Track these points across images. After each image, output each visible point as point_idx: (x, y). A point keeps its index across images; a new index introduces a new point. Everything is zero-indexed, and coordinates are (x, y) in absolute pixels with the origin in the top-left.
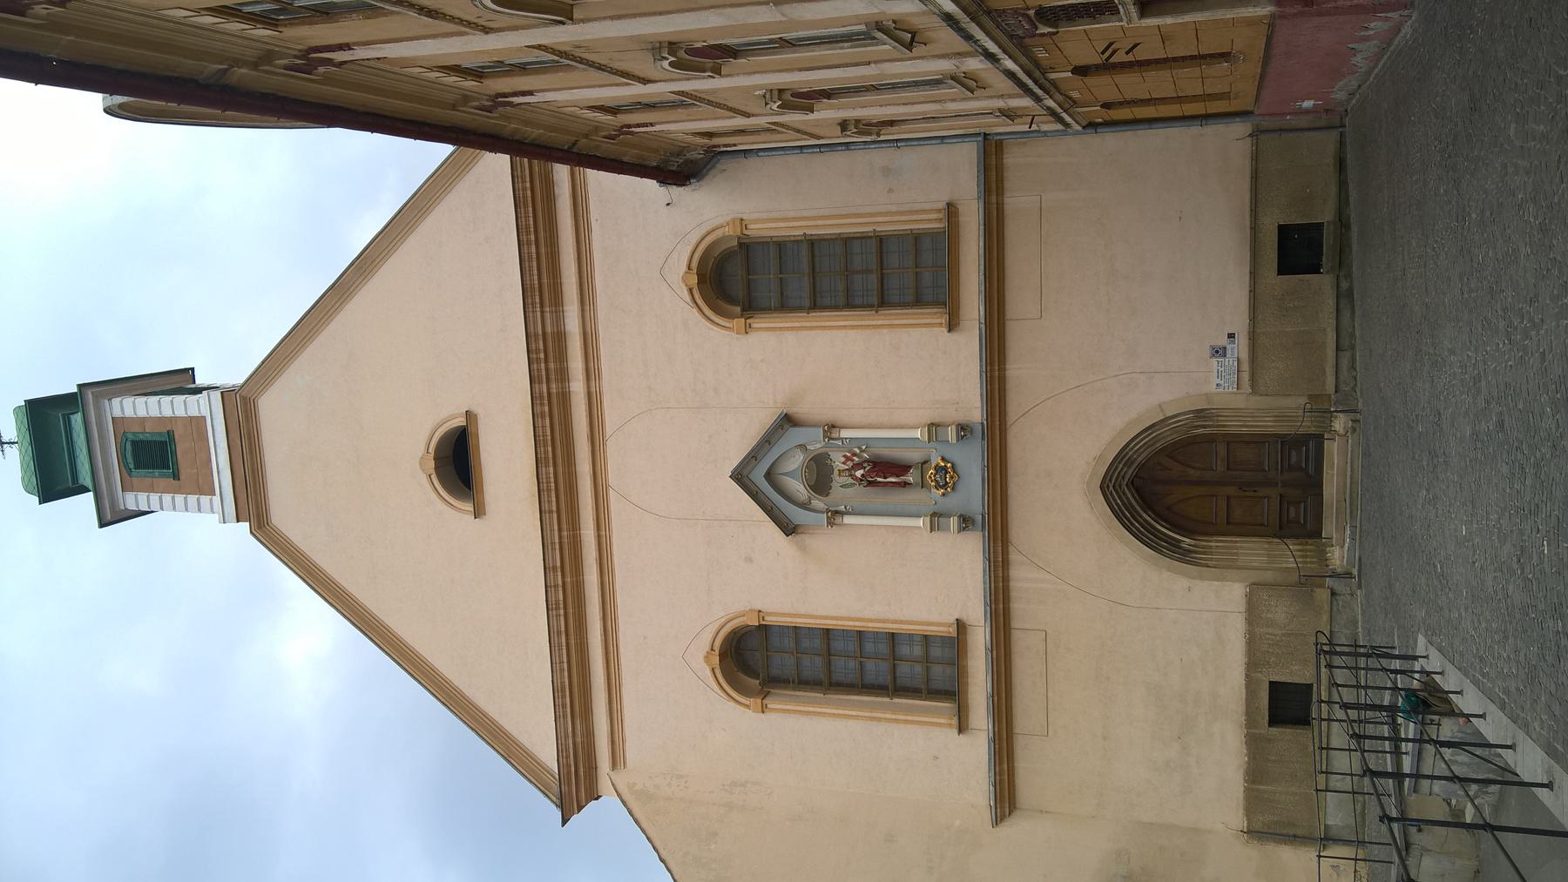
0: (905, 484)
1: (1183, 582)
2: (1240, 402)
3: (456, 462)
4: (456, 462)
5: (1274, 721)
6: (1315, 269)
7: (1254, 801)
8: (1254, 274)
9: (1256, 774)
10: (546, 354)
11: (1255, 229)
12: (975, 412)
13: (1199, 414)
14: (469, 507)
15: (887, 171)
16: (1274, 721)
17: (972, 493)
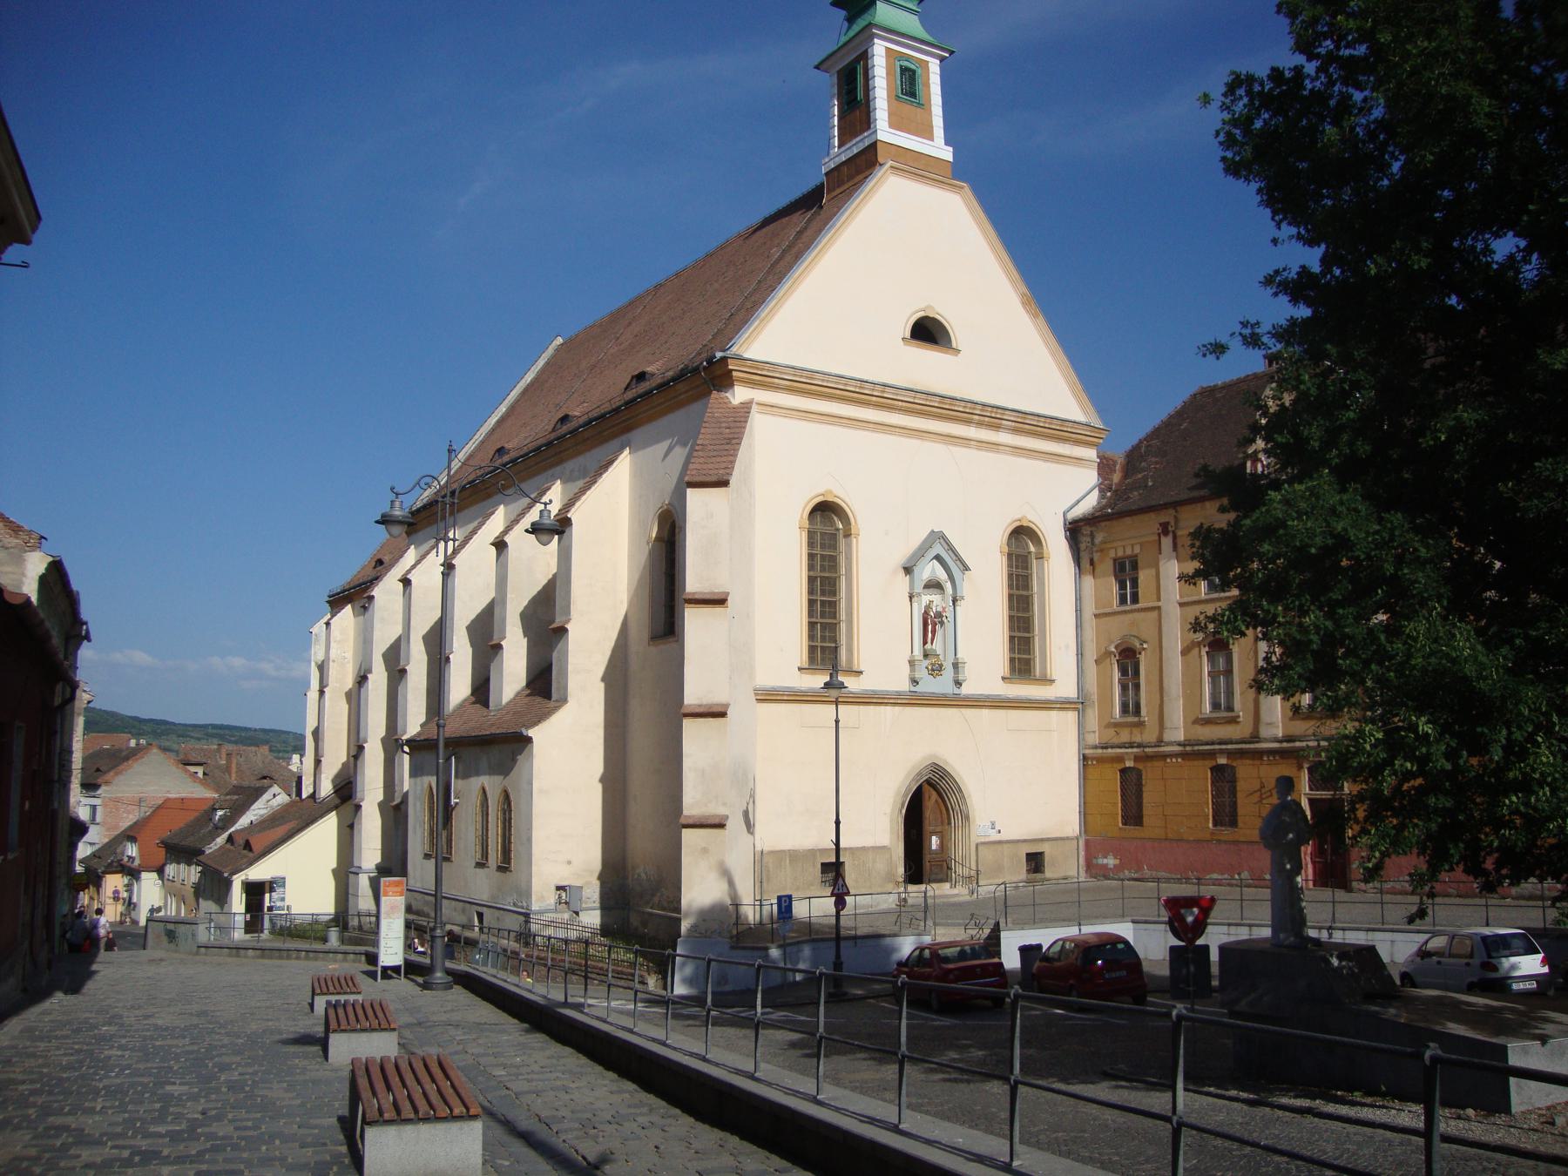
0: (925, 643)
1: (888, 811)
2: (974, 839)
3: (927, 332)
4: (927, 332)
5: (823, 864)
6: (1028, 871)
7: (779, 855)
8: (1025, 841)
9: (794, 856)
10: (991, 416)
11: (1042, 840)
12: (966, 690)
13: (966, 818)
14: (908, 334)
15: (1067, 647)
16: (823, 864)
17: (929, 685)
